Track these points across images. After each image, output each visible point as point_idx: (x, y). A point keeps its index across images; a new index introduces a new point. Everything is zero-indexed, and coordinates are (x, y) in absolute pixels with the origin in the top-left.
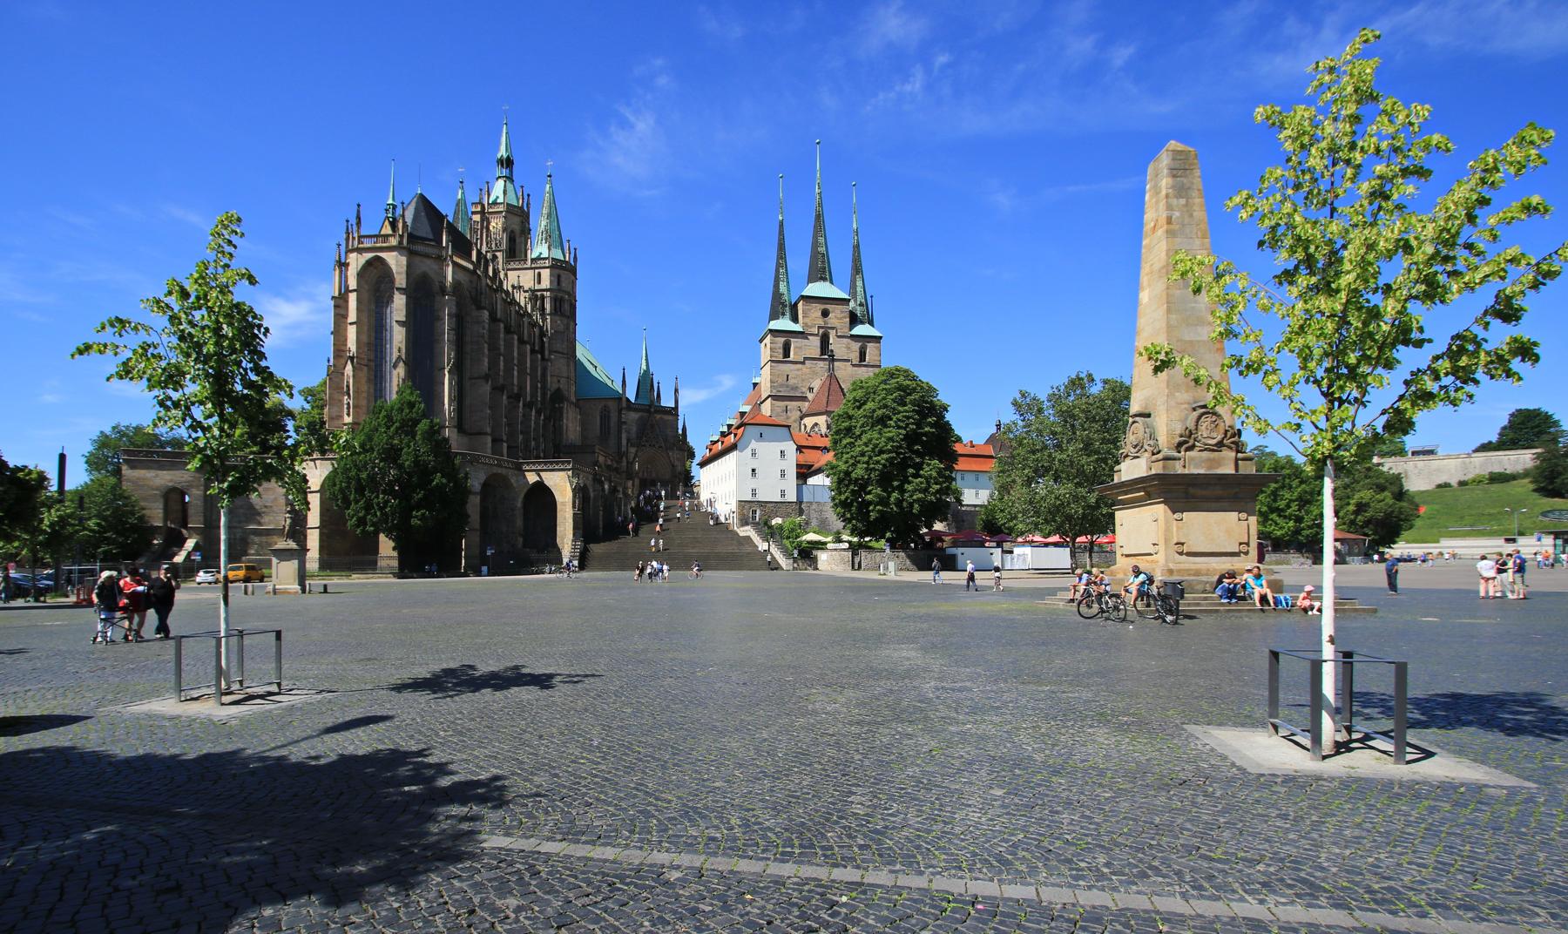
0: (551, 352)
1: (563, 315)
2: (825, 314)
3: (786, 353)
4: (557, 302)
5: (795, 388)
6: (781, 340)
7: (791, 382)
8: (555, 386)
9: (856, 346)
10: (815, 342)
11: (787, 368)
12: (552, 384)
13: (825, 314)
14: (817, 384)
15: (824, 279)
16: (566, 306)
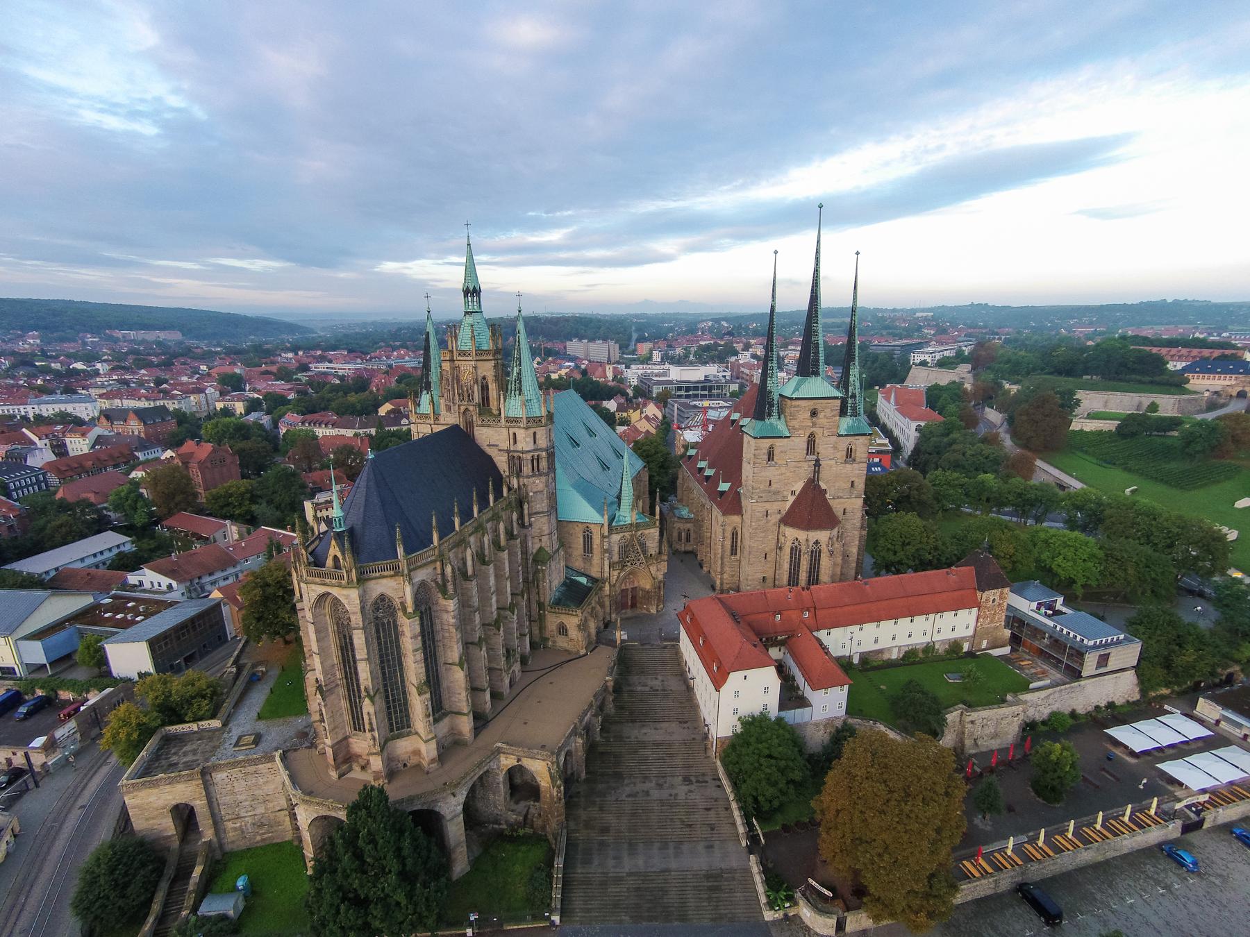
0: (530, 515)
1: (541, 475)
2: (814, 413)
3: (770, 456)
4: (535, 461)
5: (777, 493)
6: (766, 443)
7: (774, 487)
8: (537, 546)
9: (844, 443)
10: (800, 442)
11: (771, 473)
12: (533, 547)
13: (814, 413)
14: (798, 487)
15: (816, 374)
16: (544, 464)
